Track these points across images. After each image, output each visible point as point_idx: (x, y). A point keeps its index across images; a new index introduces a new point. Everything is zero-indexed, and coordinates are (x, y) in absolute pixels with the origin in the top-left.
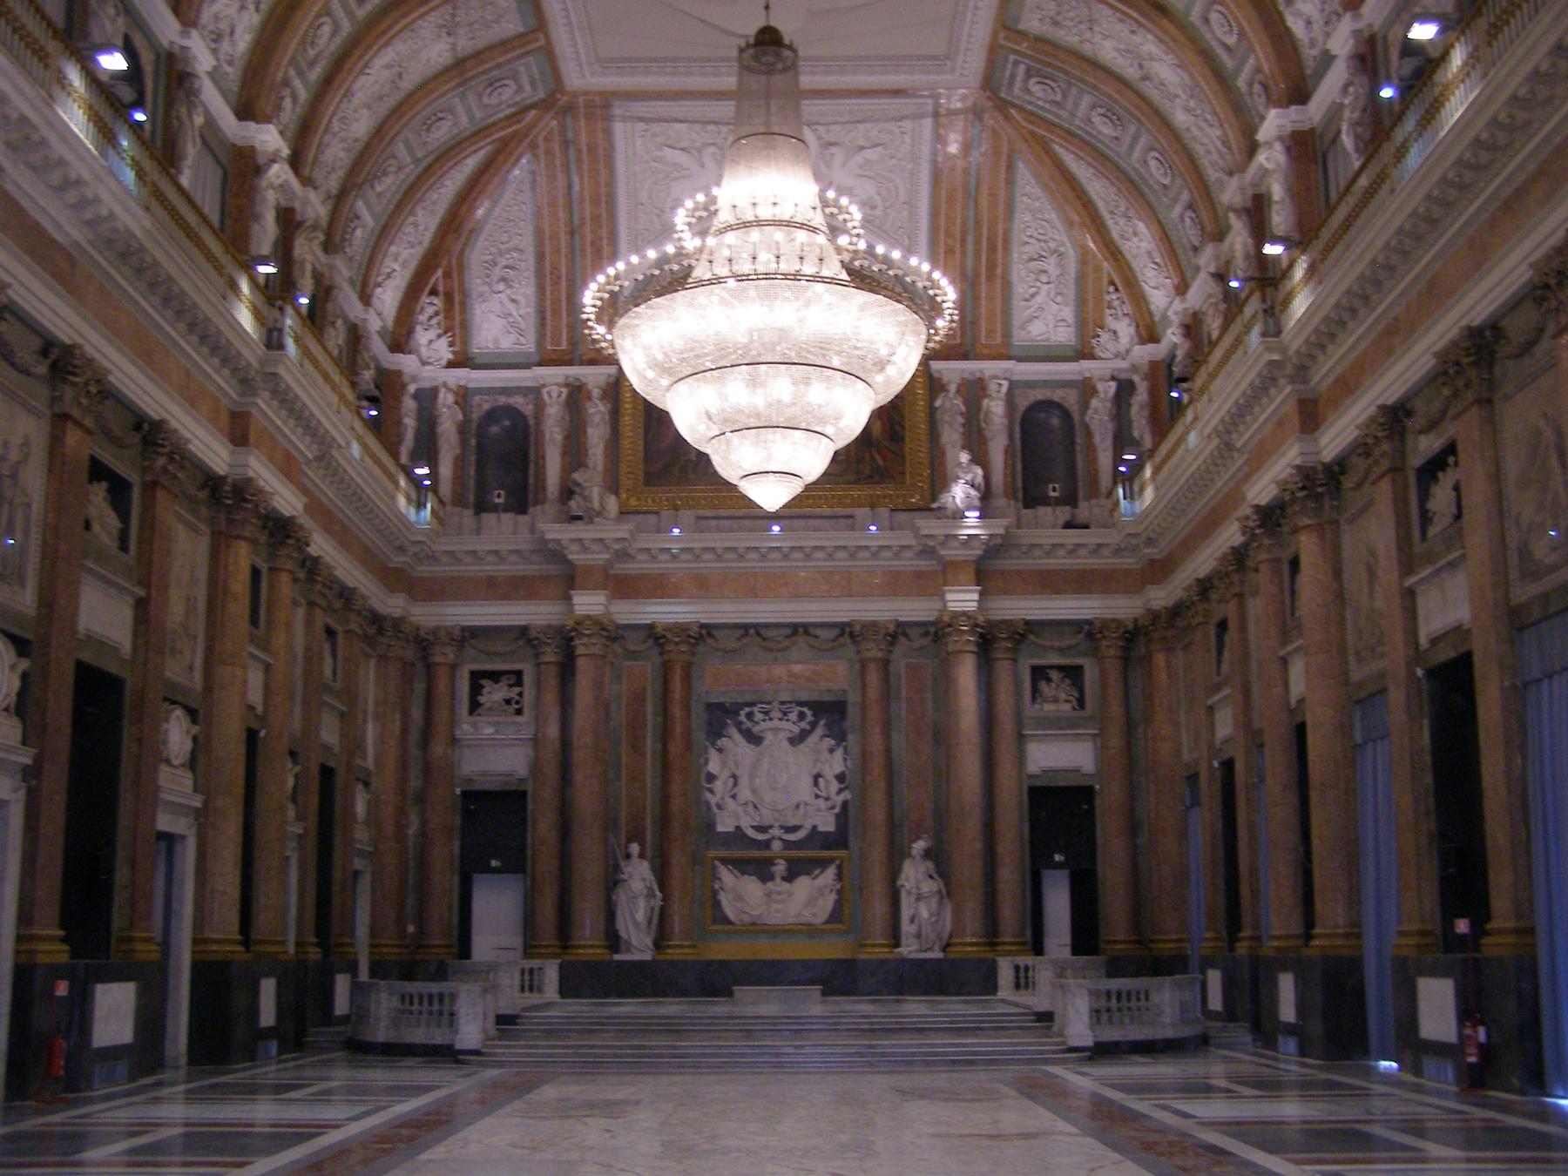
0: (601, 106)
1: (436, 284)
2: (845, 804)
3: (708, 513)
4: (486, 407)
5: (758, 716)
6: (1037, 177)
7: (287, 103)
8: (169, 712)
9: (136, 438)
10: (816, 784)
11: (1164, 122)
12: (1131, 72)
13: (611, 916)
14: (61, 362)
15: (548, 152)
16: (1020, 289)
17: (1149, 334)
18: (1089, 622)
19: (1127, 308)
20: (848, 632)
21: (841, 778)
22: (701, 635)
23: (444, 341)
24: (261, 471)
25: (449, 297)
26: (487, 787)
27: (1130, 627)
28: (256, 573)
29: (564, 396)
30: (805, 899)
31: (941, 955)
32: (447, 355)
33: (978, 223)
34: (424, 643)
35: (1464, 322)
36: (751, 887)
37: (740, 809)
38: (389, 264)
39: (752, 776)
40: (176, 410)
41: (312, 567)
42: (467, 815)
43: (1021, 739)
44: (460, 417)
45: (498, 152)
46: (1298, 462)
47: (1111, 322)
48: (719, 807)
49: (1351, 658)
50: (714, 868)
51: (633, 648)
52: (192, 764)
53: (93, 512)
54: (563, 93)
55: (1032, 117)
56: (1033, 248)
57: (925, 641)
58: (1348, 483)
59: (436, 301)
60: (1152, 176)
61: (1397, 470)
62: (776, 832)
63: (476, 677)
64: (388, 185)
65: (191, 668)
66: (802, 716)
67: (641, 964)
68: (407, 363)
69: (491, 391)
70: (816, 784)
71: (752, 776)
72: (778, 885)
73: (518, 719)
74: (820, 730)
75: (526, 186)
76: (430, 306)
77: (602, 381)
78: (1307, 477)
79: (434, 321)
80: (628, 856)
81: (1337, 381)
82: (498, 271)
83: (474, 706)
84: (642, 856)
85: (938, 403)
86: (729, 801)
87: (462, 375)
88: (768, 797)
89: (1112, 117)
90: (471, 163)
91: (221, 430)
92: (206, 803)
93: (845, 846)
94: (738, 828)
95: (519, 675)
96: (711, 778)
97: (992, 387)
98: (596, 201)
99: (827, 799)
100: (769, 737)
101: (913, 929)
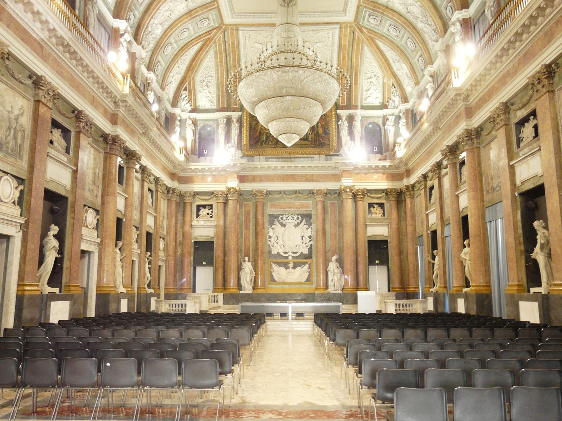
0: (236, 27)
1: (186, 87)
2: (311, 245)
3: (269, 156)
4: (202, 125)
5: (285, 218)
6: (371, 51)
7: (132, 17)
8: (86, 212)
9: (72, 115)
10: (302, 239)
11: (414, 28)
12: (402, 10)
13: (239, 279)
14: (37, 82)
15: (220, 45)
16: (365, 88)
17: (405, 100)
18: (386, 190)
19: (398, 93)
20: (311, 193)
21: (310, 237)
22: (267, 194)
23: (189, 105)
24: (121, 133)
25: (190, 92)
26: (202, 240)
27: (399, 191)
28: (121, 168)
29: (225, 121)
30: (299, 274)
31: (341, 292)
32: (190, 109)
33: (351, 67)
34: (181, 196)
35: (543, 63)
36: (282, 270)
37: (279, 247)
38: (170, 79)
39: (283, 237)
40: (89, 109)
41: (143, 169)
42: (196, 249)
43: (366, 225)
44: (194, 128)
45: (204, 45)
46: (465, 128)
47: (392, 97)
48: (272, 246)
49: (485, 193)
50: (271, 265)
51: (246, 197)
52: (97, 228)
53: (54, 139)
54: (224, 25)
55: (370, 31)
56: (369, 75)
57: (336, 195)
58: (484, 133)
59: (186, 92)
60: (408, 48)
61: (507, 125)
62: (290, 254)
63: (199, 207)
64: (169, 51)
65: (97, 196)
66: (298, 218)
67: (248, 295)
68: (177, 111)
69: (203, 120)
70: (302, 239)
71: (283, 237)
72: (290, 270)
73: (211, 219)
74: (304, 222)
75: (213, 56)
76: (184, 94)
77: (237, 116)
78: (468, 133)
79: (185, 99)
80: (245, 261)
81: (479, 100)
82: (205, 83)
83: (198, 215)
84: (249, 261)
85: (339, 123)
86: (276, 244)
87: (194, 115)
88: (288, 243)
89: (396, 28)
90: (196, 48)
91: (108, 119)
92: (102, 241)
95: (211, 206)
96: (270, 237)
97: (356, 118)
98: (234, 61)
100: (288, 225)
101: (332, 284)
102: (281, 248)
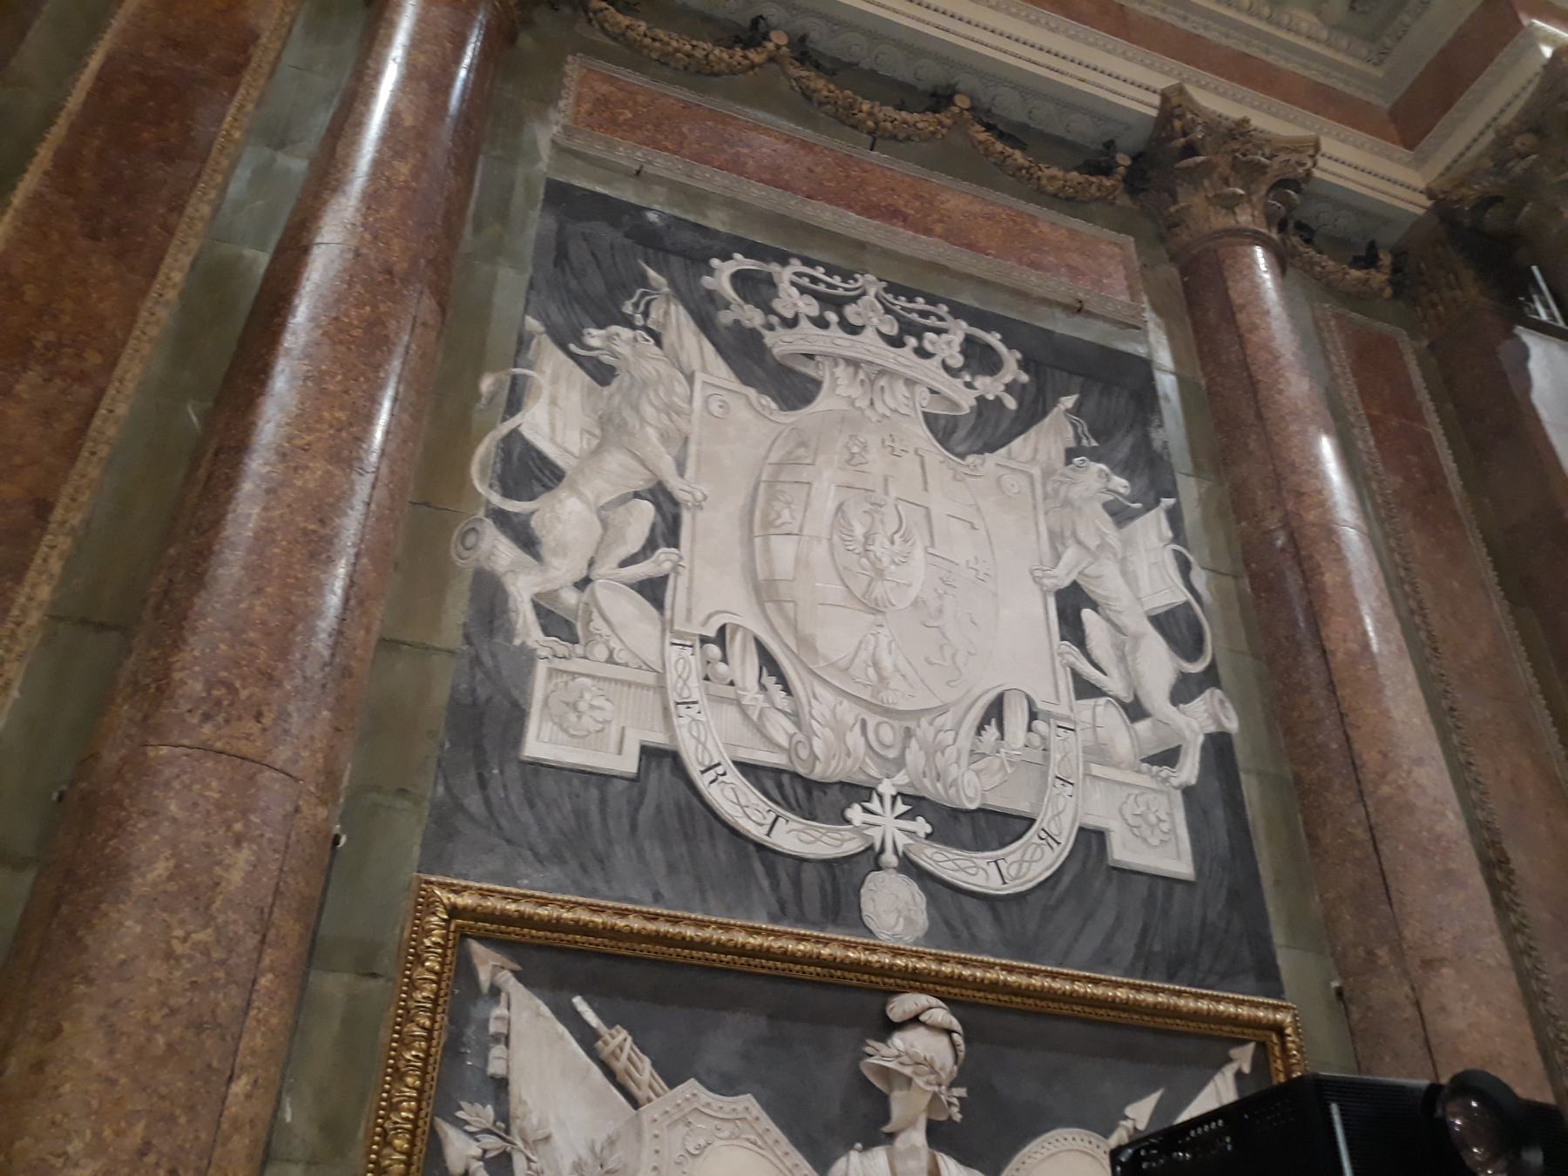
2: (1218, 747)
5: (790, 299)
10: (1072, 629)
21: (1178, 628)
37: (684, 666)
48: (554, 621)
50: (462, 992)
66: (979, 359)
70: (1072, 629)
71: (756, 524)
86: (621, 608)
88: (839, 635)
93: (1268, 979)
94: (662, 759)
96: (530, 472)
99: (1135, 710)
100: (838, 393)
102: (724, 693)
